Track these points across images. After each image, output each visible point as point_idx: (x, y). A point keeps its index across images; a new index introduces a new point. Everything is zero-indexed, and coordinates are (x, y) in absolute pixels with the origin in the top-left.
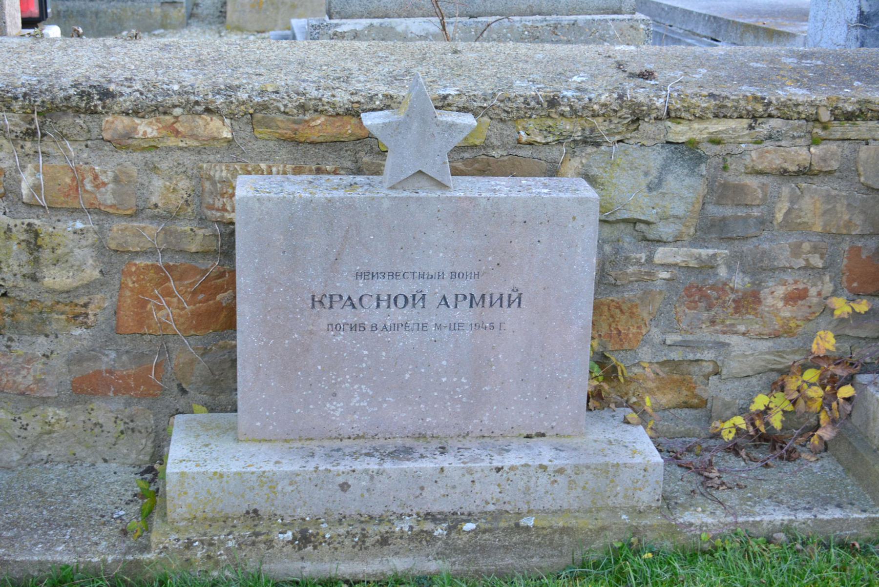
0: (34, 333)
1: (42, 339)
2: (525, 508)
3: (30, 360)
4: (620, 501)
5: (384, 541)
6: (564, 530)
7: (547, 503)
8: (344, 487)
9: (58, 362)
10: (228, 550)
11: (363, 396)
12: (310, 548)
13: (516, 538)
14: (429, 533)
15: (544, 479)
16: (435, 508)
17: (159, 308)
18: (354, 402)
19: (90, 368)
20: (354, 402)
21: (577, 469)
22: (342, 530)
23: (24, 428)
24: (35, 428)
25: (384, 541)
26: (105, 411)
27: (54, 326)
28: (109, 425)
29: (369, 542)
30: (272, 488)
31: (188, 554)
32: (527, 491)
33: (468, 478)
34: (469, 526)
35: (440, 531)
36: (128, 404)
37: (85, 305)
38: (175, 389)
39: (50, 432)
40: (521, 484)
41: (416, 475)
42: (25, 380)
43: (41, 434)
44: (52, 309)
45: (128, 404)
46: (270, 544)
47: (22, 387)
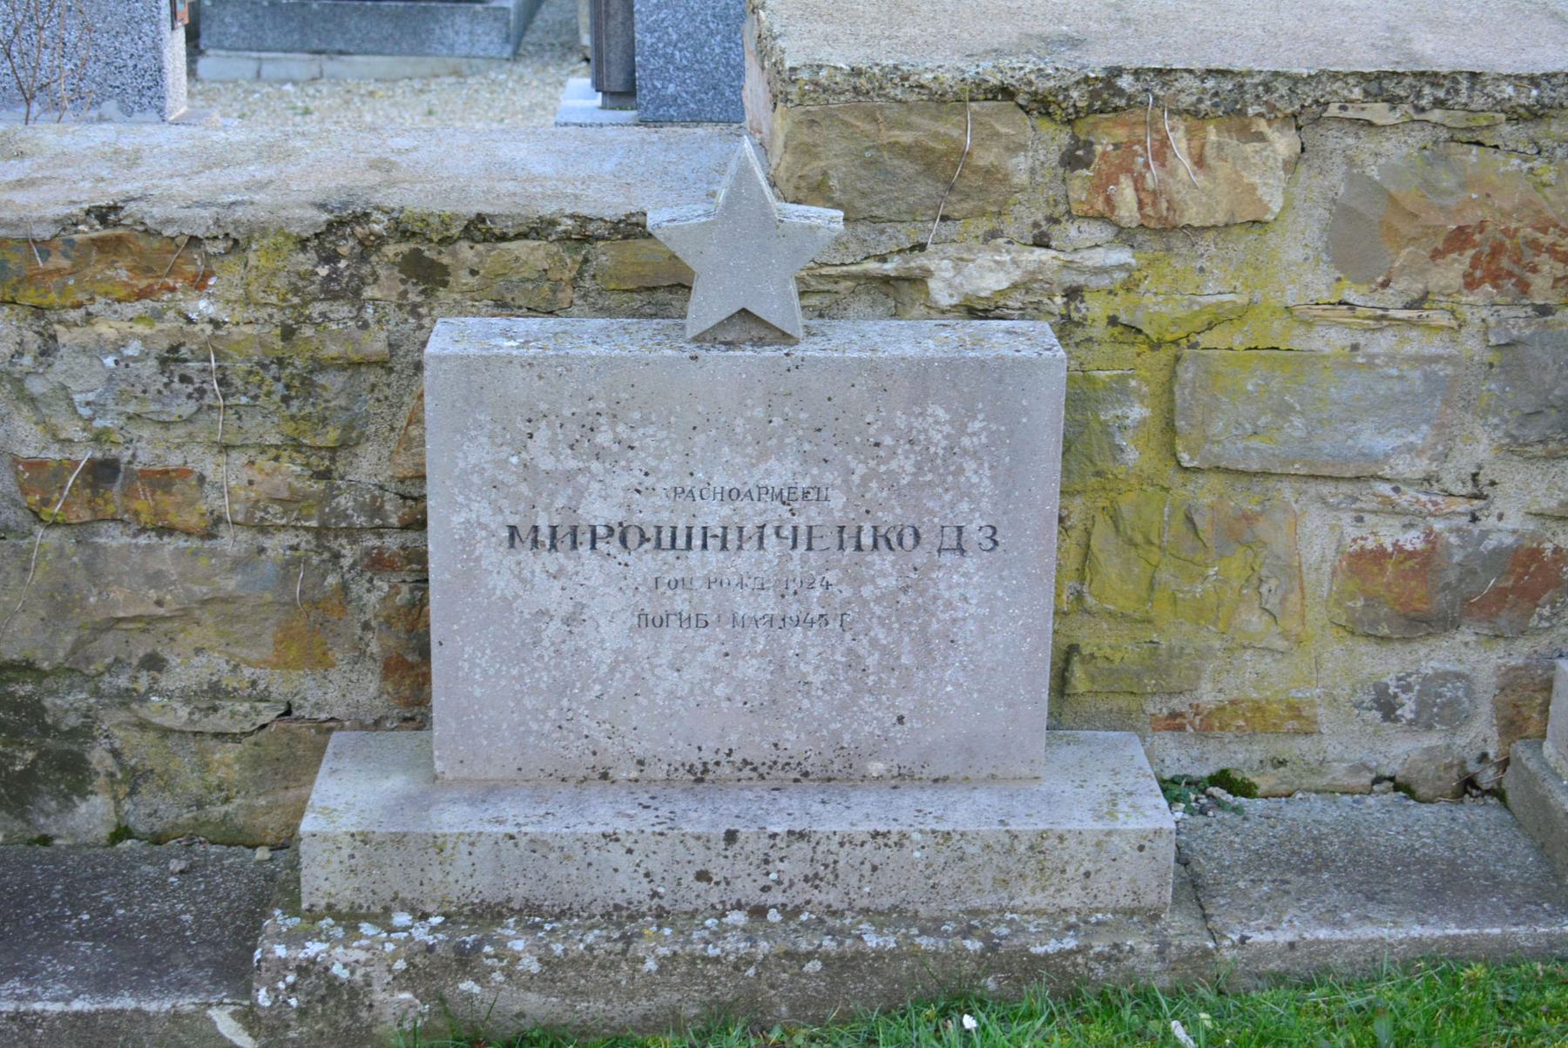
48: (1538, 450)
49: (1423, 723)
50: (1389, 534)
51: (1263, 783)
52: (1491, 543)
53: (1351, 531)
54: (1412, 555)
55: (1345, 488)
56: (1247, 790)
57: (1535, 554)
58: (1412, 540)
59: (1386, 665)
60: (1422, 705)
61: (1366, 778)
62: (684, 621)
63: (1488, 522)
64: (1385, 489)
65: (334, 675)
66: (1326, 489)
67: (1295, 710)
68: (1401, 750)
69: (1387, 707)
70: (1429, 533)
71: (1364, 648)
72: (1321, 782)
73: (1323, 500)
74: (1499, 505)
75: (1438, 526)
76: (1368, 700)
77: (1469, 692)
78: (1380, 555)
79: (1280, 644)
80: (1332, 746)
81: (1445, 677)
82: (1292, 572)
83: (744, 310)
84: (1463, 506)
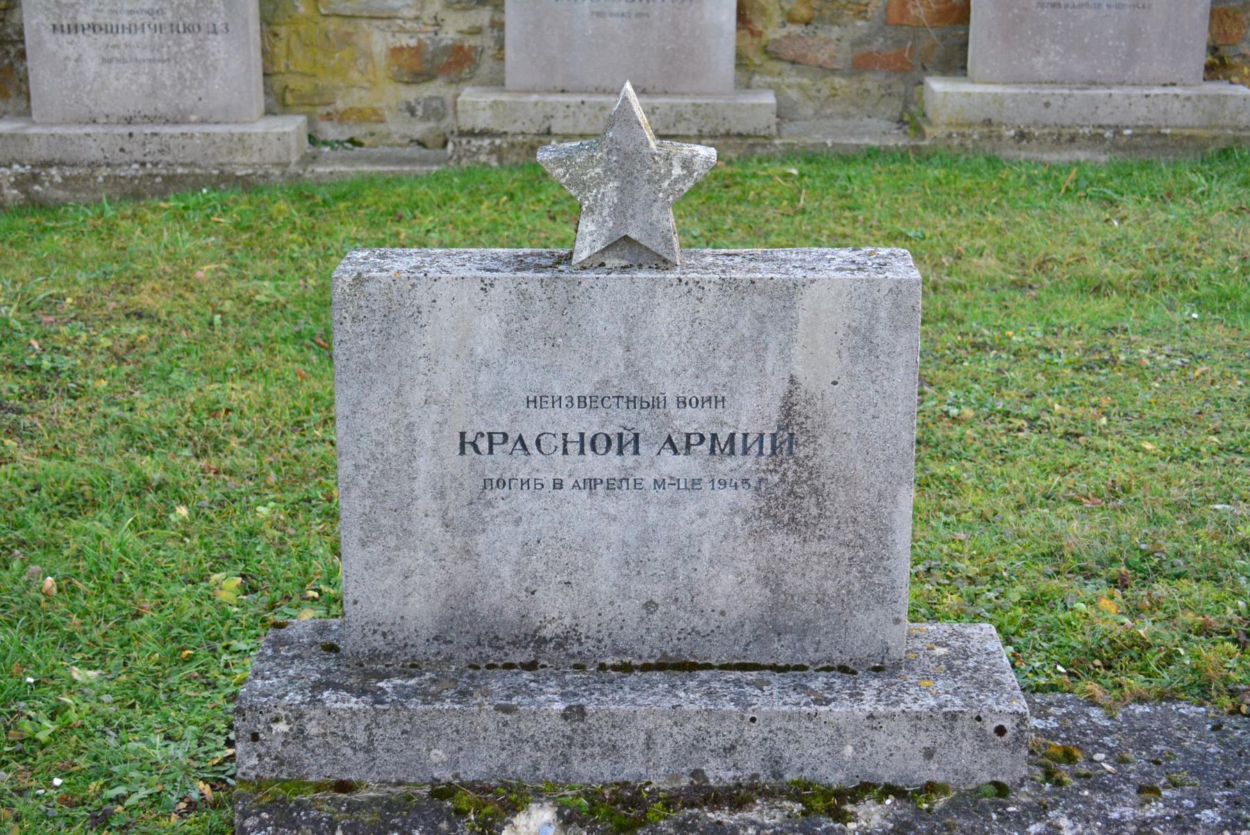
0: (832, 23)
1: (836, 28)
2: (1163, 124)
3: (828, 42)
4: (1227, 121)
5: (1072, 139)
6: (1190, 137)
7: (1179, 121)
8: (1047, 105)
9: (845, 45)
10: (974, 141)
11: (1057, 53)
12: (1024, 142)
13: (1158, 142)
14: (1101, 135)
15: (1177, 104)
16: (1104, 122)
17: (915, 7)
18: (1052, 57)
19: (865, 49)
20: (1052, 57)
21: (1199, 97)
22: (1046, 131)
23: (819, 91)
24: (826, 92)
25: (1072, 139)
26: (872, 82)
27: (845, 19)
28: (874, 91)
29: (1063, 140)
30: (1001, 104)
31: (949, 142)
32: (1165, 112)
33: (1126, 102)
34: (1127, 132)
35: (1108, 134)
36: (888, 76)
37: (867, 5)
38: (920, 68)
39: (834, 96)
40: (1162, 107)
41: (1093, 98)
42: (823, 57)
43: (829, 97)
44: (845, 7)
45: (888, 76)
46: (1000, 137)
47: (821, 62)
48: (458, 6)
49: (426, 118)
50: (406, 41)
51: (367, 141)
52: (443, 43)
53: (391, 40)
54: (412, 48)
55: (386, 22)
56: (360, 145)
57: (461, 48)
58: (413, 43)
59: (411, 94)
60: (425, 110)
61: (407, 141)
62: (118, 61)
63: (442, 35)
64: (400, 22)
65: (11, 101)
66: (379, 23)
67: (375, 112)
68: (419, 129)
69: (412, 111)
70: (419, 41)
71: (402, 87)
72: (390, 142)
73: (377, 27)
74: (446, 28)
75: (422, 36)
76: (404, 107)
77: (443, 103)
78: (401, 49)
79: (367, 85)
80: (393, 128)
81: (431, 98)
82: (369, 56)
83: (626, 236)
84: (430, 29)
